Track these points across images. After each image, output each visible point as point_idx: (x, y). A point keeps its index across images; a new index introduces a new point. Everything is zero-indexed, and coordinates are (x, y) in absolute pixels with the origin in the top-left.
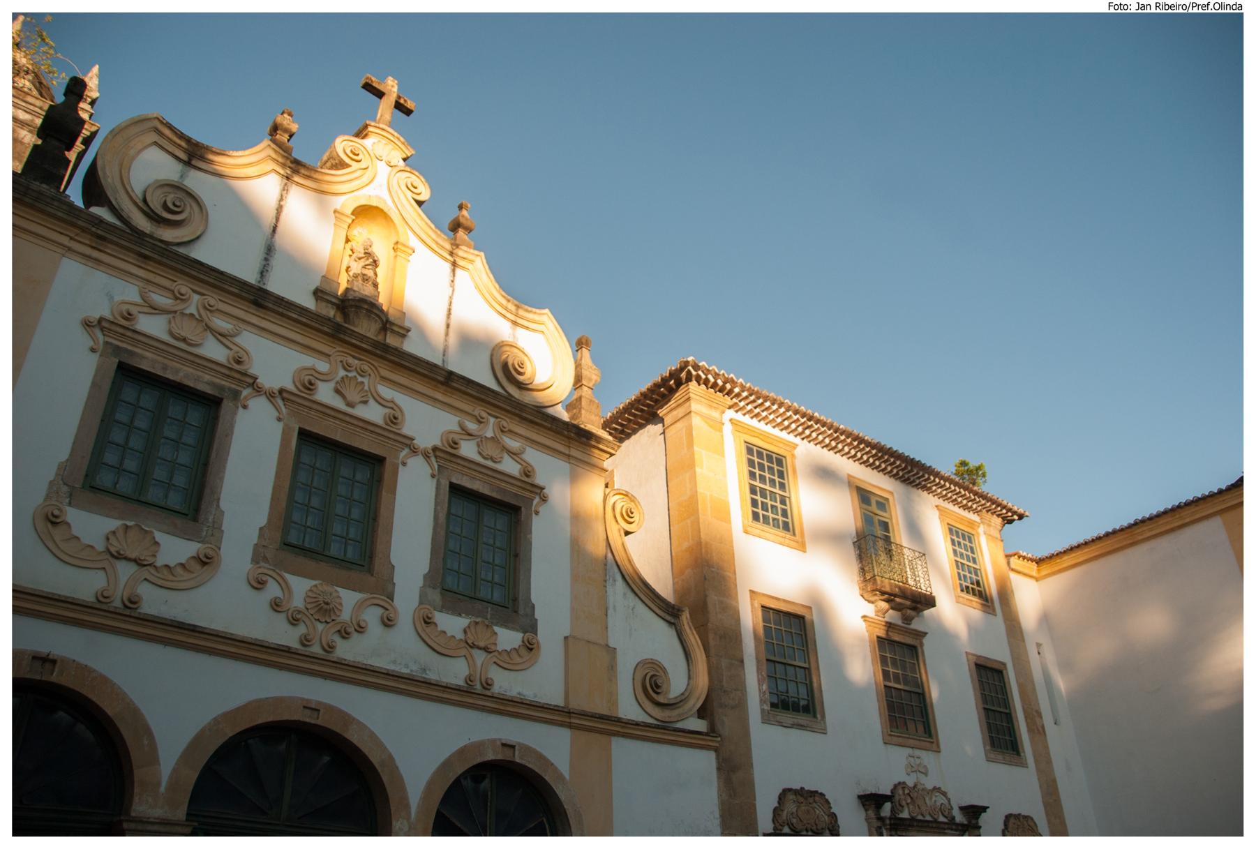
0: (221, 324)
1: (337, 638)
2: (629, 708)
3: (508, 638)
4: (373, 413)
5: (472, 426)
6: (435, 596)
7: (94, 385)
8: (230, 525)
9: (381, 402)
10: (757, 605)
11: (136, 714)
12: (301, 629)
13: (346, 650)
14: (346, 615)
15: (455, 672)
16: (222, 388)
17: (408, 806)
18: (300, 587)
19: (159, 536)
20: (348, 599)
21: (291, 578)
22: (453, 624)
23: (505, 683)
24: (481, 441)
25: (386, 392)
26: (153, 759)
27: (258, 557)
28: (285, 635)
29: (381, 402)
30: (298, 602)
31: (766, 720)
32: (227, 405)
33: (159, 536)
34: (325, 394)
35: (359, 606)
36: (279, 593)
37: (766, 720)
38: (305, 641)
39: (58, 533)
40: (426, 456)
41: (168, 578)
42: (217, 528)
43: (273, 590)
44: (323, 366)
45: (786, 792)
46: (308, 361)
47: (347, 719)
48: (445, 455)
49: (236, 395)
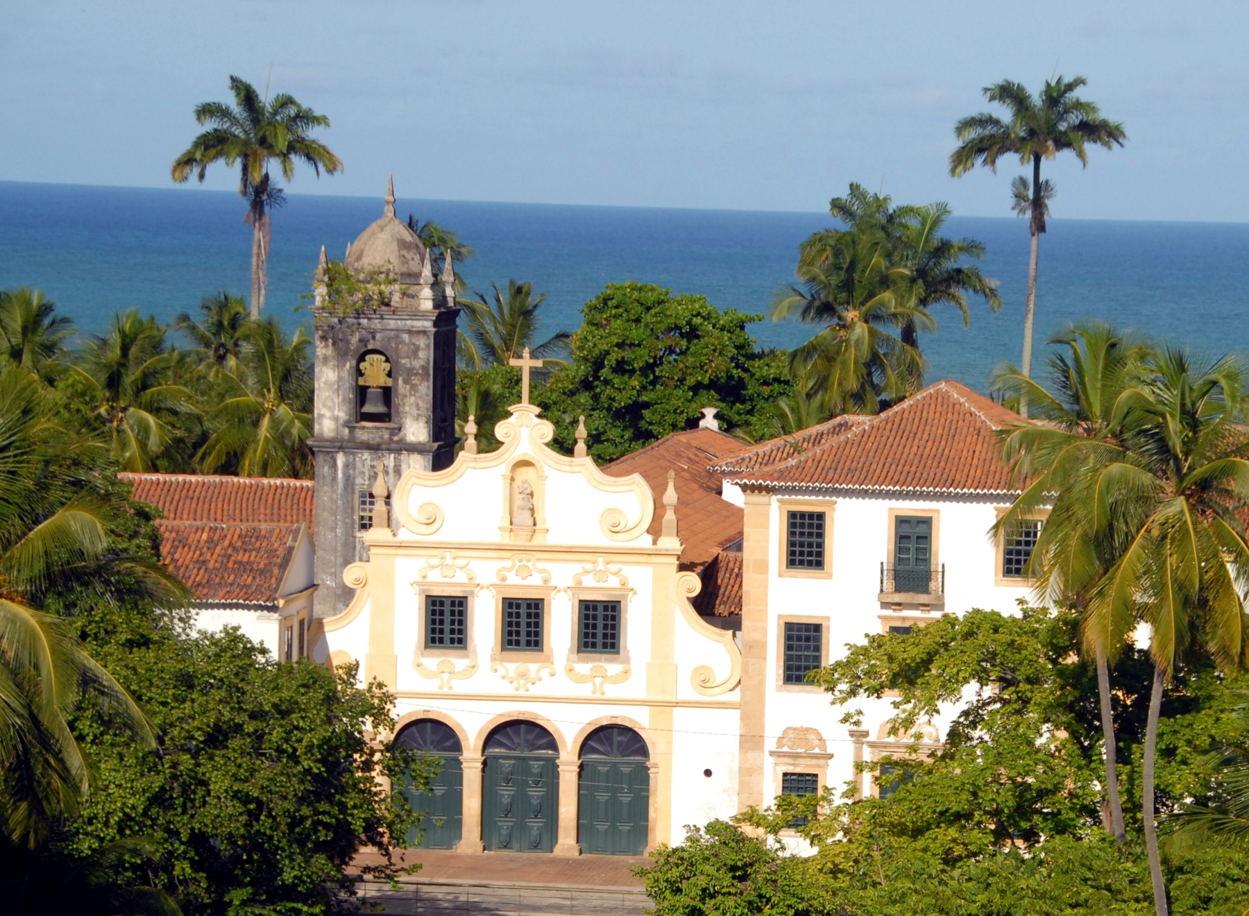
0: (461, 562)
1: (529, 685)
2: (687, 691)
5: (589, 566)
6: (575, 656)
7: (420, 609)
8: (479, 650)
9: (540, 571)
11: (458, 725)
12: (515, 684)
13: (534, 691)
14: (533, 675)
15: (585, 690)
16: (466, 592)
17: (566, 746)
21: (507, 664)
23: (612, 691)
24: (596, 573)
25: (540, 565)
26: (467, 739)
27: (493, 659)
28: (508, 690)
29: (540, 571)
30: (512, 674)
31: (778, 689)
34: (513, 579)
35: (539, 670)
36: (504, 673)
37: (778, 689)
38: (517, 689)
40: (566, 591)
42: (475, 651)
44: (508, 564)
45: (788, 728)
47: (537, 716)
49: (472, 593)
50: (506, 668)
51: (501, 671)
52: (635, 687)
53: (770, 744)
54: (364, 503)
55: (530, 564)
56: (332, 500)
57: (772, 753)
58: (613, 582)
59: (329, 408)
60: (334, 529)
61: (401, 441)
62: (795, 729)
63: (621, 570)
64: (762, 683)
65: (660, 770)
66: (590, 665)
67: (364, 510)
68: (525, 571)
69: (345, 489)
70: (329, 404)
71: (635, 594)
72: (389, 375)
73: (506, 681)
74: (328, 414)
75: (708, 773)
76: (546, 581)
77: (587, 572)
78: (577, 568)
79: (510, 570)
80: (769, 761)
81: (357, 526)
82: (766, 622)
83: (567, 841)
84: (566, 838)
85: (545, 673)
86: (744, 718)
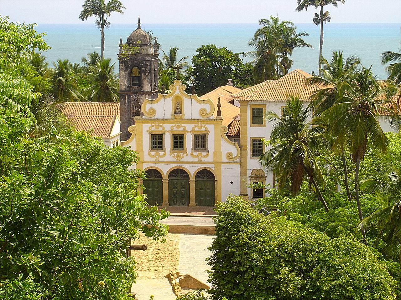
3: (204, 154)
4: (182, 129)
5: (196, 125)
6: (193, 151)
10: (251, 139)
12: (176, 159)
13: (182, 160)
14: (181, 156)
15: (196, 160)
18: (175, 154)
19: (159, 153)
20: (182, 154)
22: (196, 154)
23: (203, 160)
25: (183, 125)
27: (170, 152)
28: (175, 160)
30: (176, 156)
31: (251, 158)
32: (163, 135)
33: (159, 153)
35: (184, 154)
37: (251, 158)
39: (150, 155)
41: (161, 157)
43: (173, 155)
44: (174, 125)
46: (171, 125)
48: (193, 131)
50: (174, 155)
51: (173, 155)
52: (210, 158)
53: (249, 174)
54: (134, 109)
55: (180, 125)
56: (124, 108)
57: (249, 176)
58: (203, 129)
59: (123, 83)
60: (125, 117)
61: (143, 91)
62: (256, 170)
63: (205, 126)
64: (246, 157)
65: (218, 182)
66: (198, 153)
67: (134, 111)
68: (178, 127)
69: (128, 105)
70: (123, 81)
71: (210, 132)
72: (139, 73)
73: (174, 158)
74: (123, 84)
75: (232, 183)
76: (184, 130)
77: (196, 127)
78: (193, 125)
79: (174, 126)
80: (249, 179)
81: (132, 116)
82: (247, 139)
83: (193, 202)
84: (192, 202)
85: (185, 155)
86: (242, 167)
